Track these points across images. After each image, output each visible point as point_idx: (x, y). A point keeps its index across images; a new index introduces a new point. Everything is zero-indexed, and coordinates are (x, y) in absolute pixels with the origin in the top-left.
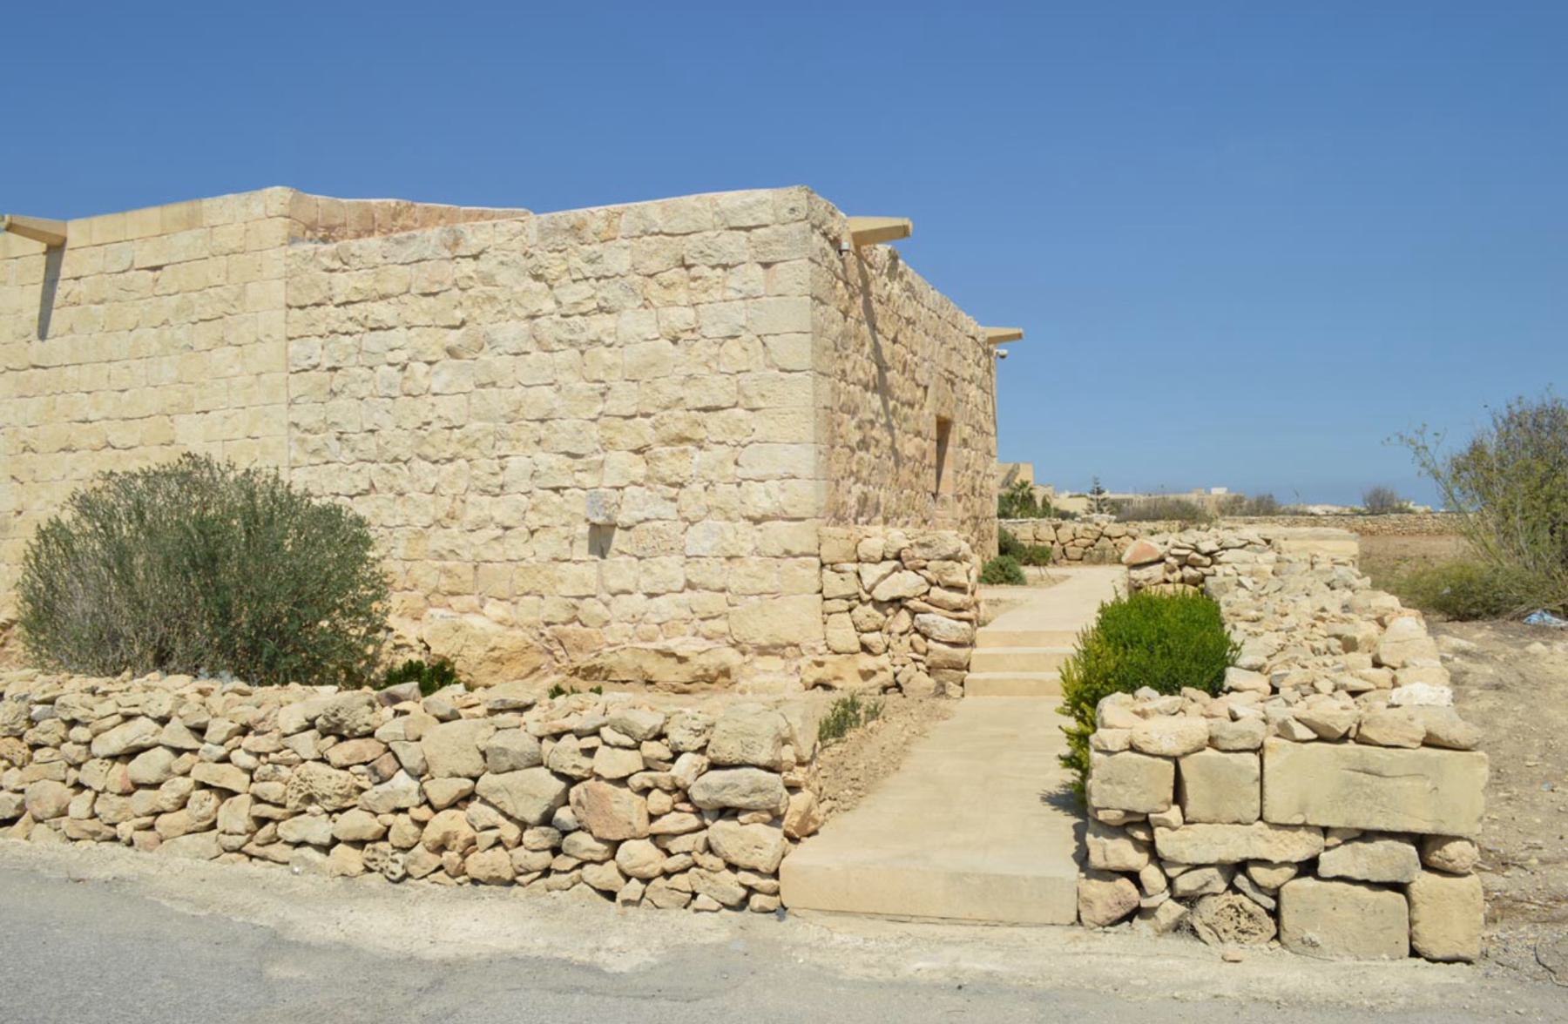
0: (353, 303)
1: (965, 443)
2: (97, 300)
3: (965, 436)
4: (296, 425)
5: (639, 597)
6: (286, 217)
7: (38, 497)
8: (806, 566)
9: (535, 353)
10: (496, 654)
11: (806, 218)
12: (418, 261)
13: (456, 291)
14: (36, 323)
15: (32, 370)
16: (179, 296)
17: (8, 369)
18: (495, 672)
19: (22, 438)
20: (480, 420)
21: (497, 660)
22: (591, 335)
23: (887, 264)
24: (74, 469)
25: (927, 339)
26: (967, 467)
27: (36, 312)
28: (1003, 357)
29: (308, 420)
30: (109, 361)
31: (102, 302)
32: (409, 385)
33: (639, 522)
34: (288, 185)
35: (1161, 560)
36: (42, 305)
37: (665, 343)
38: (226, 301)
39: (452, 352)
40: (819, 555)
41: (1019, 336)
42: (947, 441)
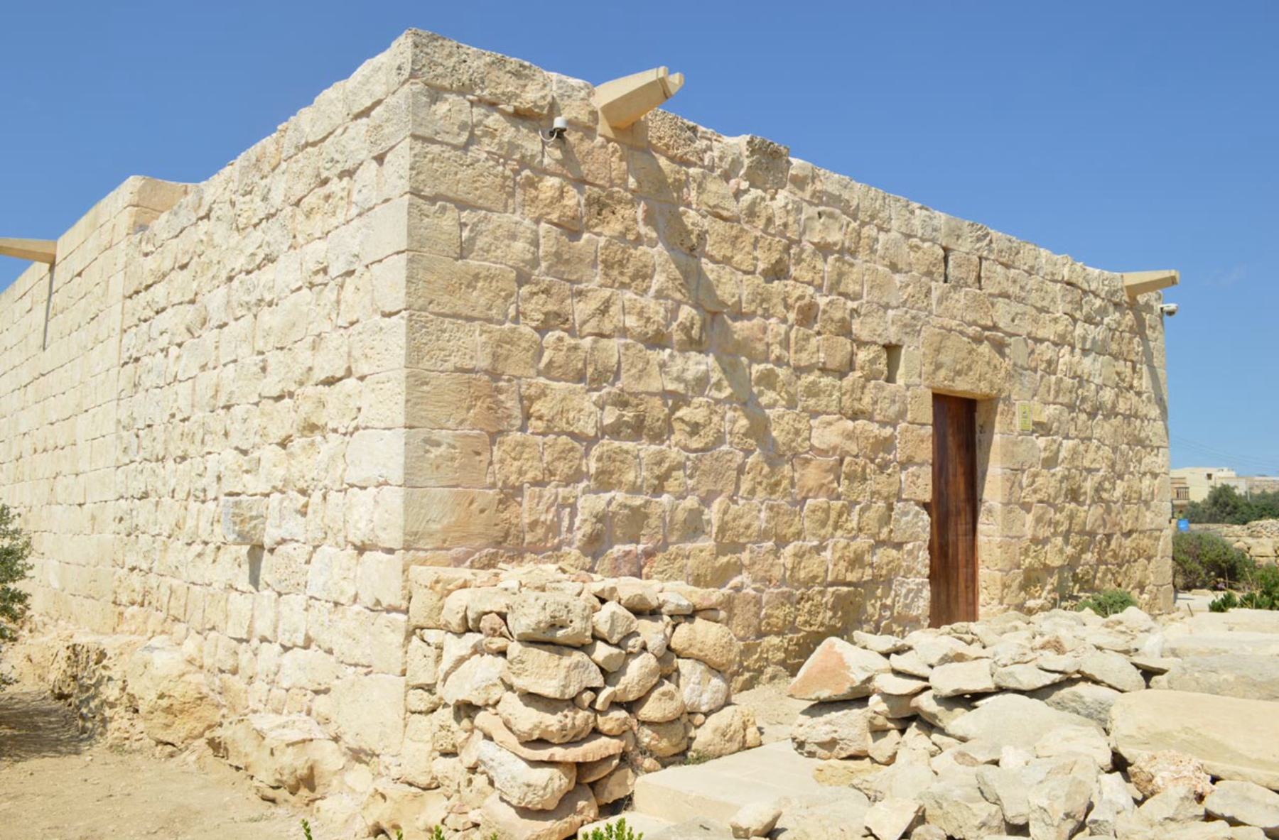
1: (1042, 428)
3: (1044, 419)
5: (276, 648)
6: (134, 206)
8: (391, 626)
10: (165, 703)
11: (413, 75)
12: (181, 232)
18: (168, 726)
21: (168, 710)
23: (746, 162)
25: (898, 279)
26: (1050, 463)
28: (1171, 313)
33: (279, 544)
34: (139, 174)
35: (859, 698)
37: (305, 291)
40: (407, 611)
41: (1173, 281)
42: (993, 427)
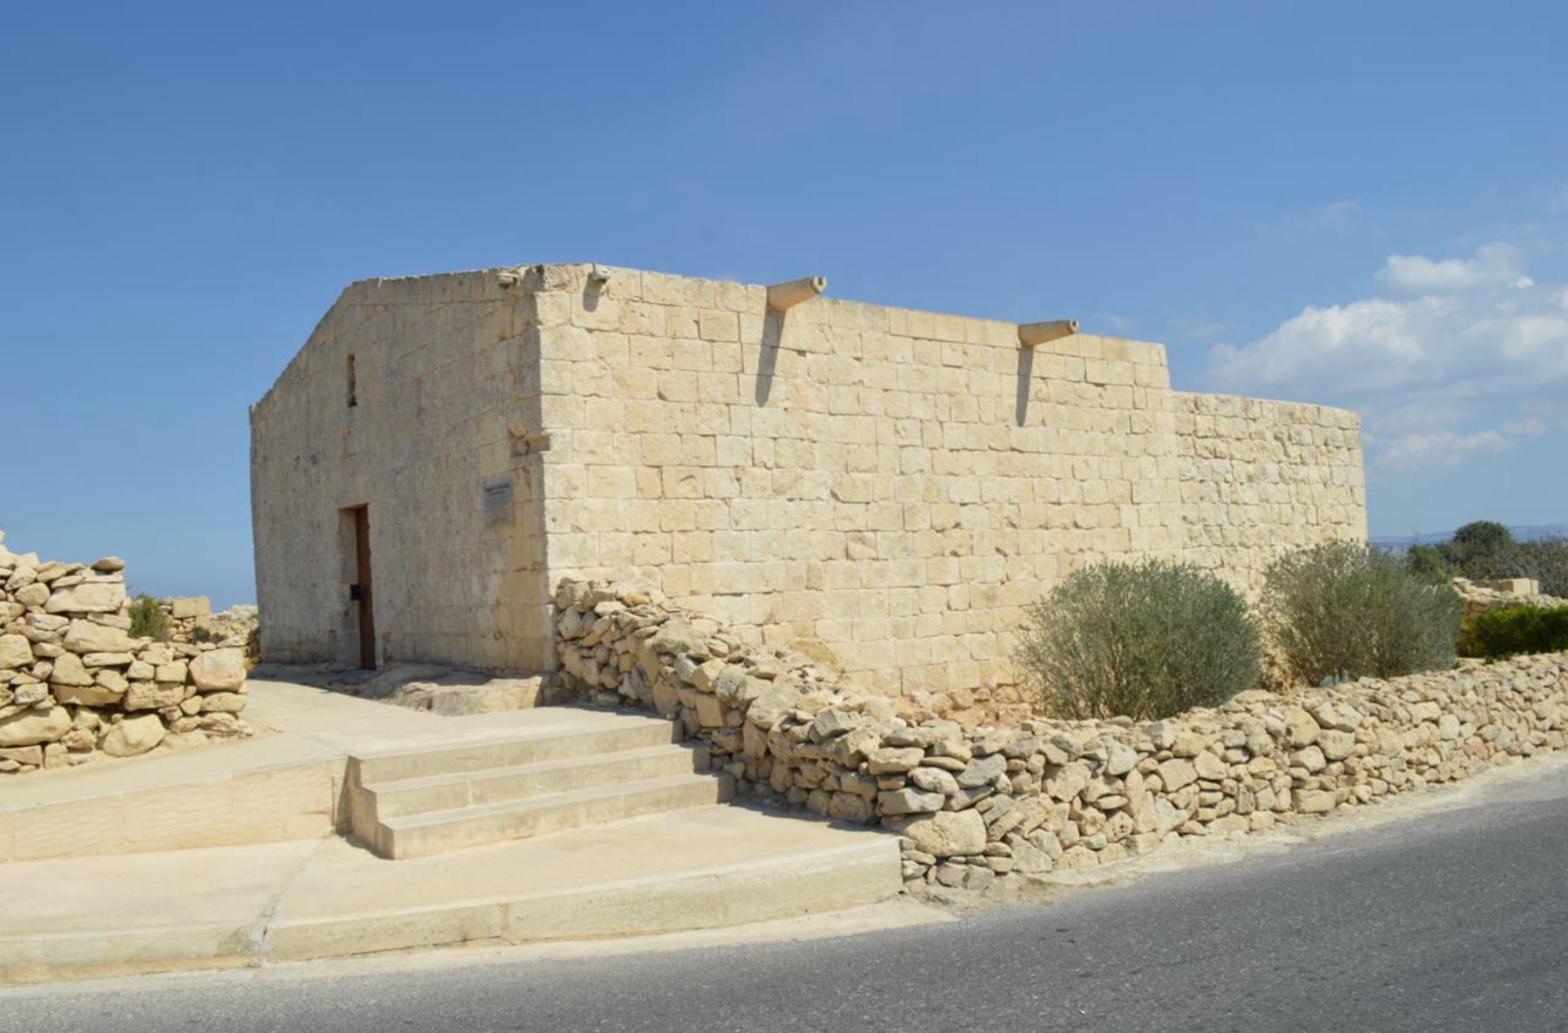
0: (1206, 437)
2: (1062, 401)
4: (1185, 518)
7: (1022, 568)
9: (1281, 486)
13: (1249, 440)
14: (1014, 412)
15: (1010, 452)
16: (1116, 411)
17: (991, 448)
19: (1006, 514)
20: (1263, 522)
22: (1300, 477)
24: (1052, 545)
27: (1013, 401)
29: (1192, 516)
30: (1073, 454)
31: (1065, 403)
32: (1235, 497)
36: (1018, 396)
38: (1145, 421)
39: (1250, 479)
